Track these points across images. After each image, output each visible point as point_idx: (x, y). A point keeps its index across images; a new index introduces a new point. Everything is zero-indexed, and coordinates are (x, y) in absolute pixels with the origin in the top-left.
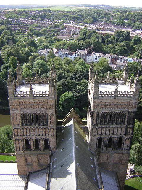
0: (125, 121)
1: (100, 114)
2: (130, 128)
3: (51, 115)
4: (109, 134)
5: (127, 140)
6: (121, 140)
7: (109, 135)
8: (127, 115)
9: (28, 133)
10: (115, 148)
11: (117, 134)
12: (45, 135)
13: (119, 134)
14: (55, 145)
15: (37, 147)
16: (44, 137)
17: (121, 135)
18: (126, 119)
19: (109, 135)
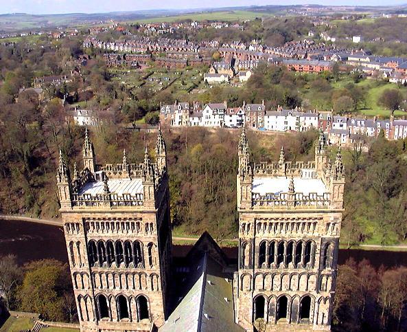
0: (314, 260)
1: (257, 244)
2: (328, 276)
3: (150, 245)
4: (279, 287)
5: (322, 301)
6: (306, 301)
7: (281, 289)
8: (319, 247)
9: (104, 282)
10: (293, 319)
11: (298, 289)
12: (141, 288)
13: (303, 288)
14: (162, 309)
15: (124, 313)
16: (137, 293)
17: (307, 290)
18: (317, 256)
19: (281, 289)
